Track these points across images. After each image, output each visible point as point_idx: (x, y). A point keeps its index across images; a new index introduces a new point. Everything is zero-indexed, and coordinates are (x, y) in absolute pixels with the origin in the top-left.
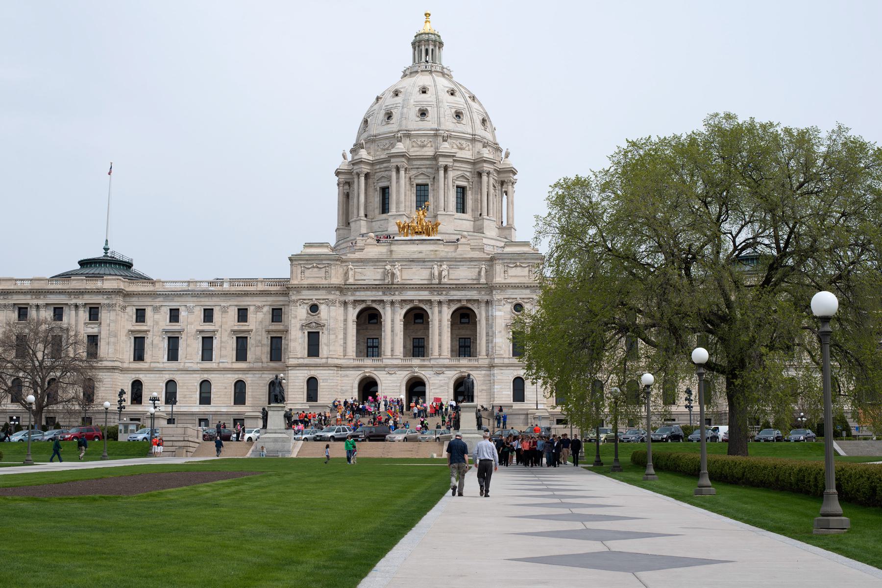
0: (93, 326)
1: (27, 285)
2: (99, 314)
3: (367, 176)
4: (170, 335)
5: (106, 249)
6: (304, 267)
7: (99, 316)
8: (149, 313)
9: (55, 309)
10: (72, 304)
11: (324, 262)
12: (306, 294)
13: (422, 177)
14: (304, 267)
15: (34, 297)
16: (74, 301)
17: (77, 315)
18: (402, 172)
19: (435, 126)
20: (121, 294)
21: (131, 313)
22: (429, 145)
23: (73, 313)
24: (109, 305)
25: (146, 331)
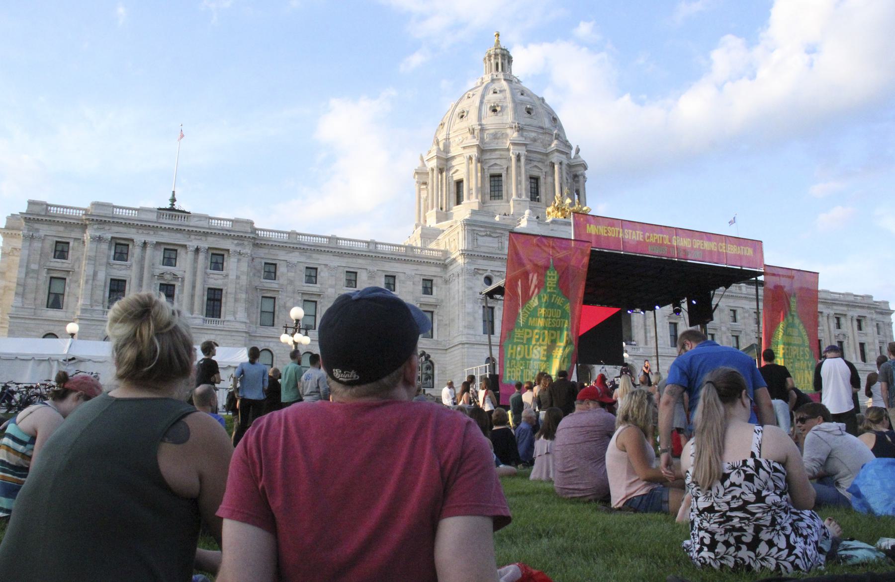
0: (216, 276)
3: (479, 160)
4: (306, 298)
5: (173, 200)
6: (477, 234)
8: (282, 269)
11: (499, 231)
12: (482, 264)
13: (535, 169)
14: (477, 234)
18: (523, 159)
19: (541, 125)
22: (539, 141)
23: (190, 256)
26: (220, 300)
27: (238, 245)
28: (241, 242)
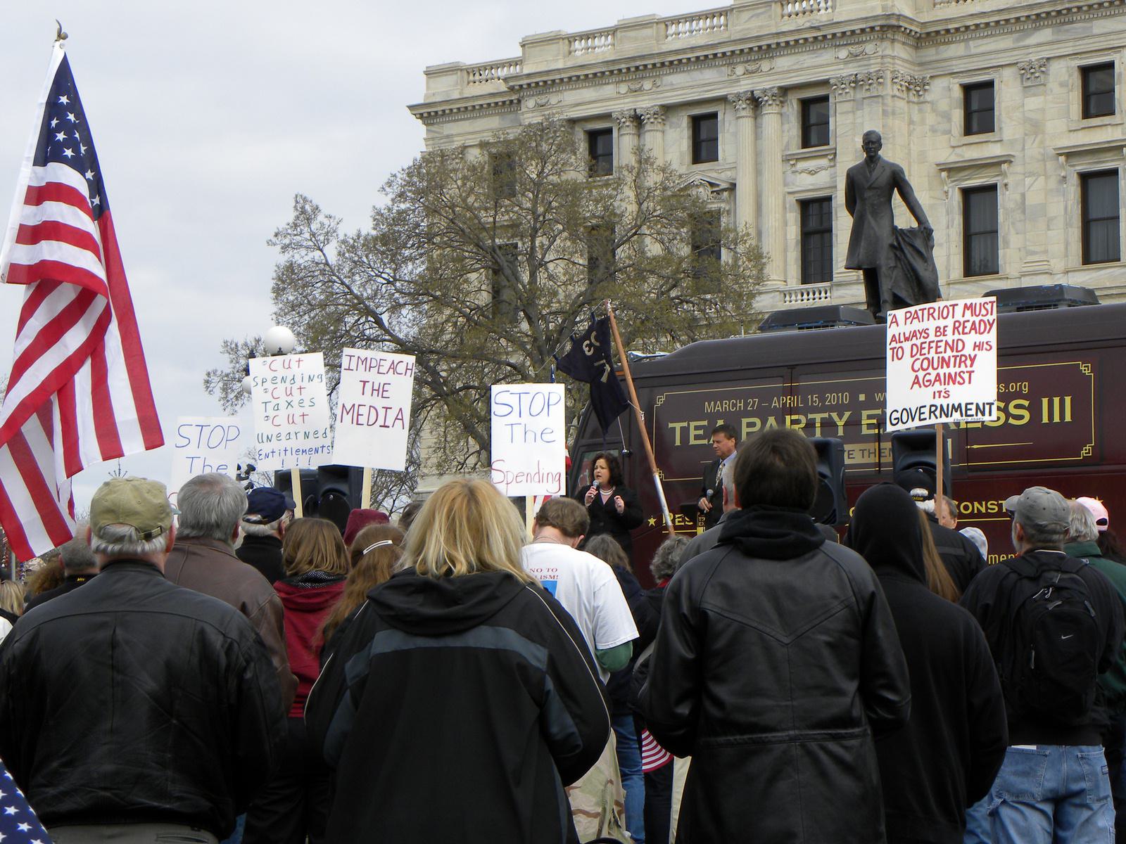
1: (603, 50)
2: (831, 120)
7: (832, 127)
8: (1007, 95)
9: (696, 122)
10: (738, 96)
15: (623, 88)
16: (745, 86)
17: (757, 128)
20: (899, 37)
21: (943, 105)
23: (747, 124)
24: (856, 82)
25: (995, 164)
26: (830, 230)
27: (854, 57)
28: (855, 49)
